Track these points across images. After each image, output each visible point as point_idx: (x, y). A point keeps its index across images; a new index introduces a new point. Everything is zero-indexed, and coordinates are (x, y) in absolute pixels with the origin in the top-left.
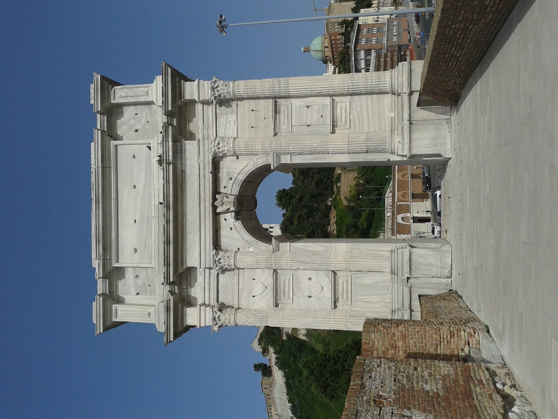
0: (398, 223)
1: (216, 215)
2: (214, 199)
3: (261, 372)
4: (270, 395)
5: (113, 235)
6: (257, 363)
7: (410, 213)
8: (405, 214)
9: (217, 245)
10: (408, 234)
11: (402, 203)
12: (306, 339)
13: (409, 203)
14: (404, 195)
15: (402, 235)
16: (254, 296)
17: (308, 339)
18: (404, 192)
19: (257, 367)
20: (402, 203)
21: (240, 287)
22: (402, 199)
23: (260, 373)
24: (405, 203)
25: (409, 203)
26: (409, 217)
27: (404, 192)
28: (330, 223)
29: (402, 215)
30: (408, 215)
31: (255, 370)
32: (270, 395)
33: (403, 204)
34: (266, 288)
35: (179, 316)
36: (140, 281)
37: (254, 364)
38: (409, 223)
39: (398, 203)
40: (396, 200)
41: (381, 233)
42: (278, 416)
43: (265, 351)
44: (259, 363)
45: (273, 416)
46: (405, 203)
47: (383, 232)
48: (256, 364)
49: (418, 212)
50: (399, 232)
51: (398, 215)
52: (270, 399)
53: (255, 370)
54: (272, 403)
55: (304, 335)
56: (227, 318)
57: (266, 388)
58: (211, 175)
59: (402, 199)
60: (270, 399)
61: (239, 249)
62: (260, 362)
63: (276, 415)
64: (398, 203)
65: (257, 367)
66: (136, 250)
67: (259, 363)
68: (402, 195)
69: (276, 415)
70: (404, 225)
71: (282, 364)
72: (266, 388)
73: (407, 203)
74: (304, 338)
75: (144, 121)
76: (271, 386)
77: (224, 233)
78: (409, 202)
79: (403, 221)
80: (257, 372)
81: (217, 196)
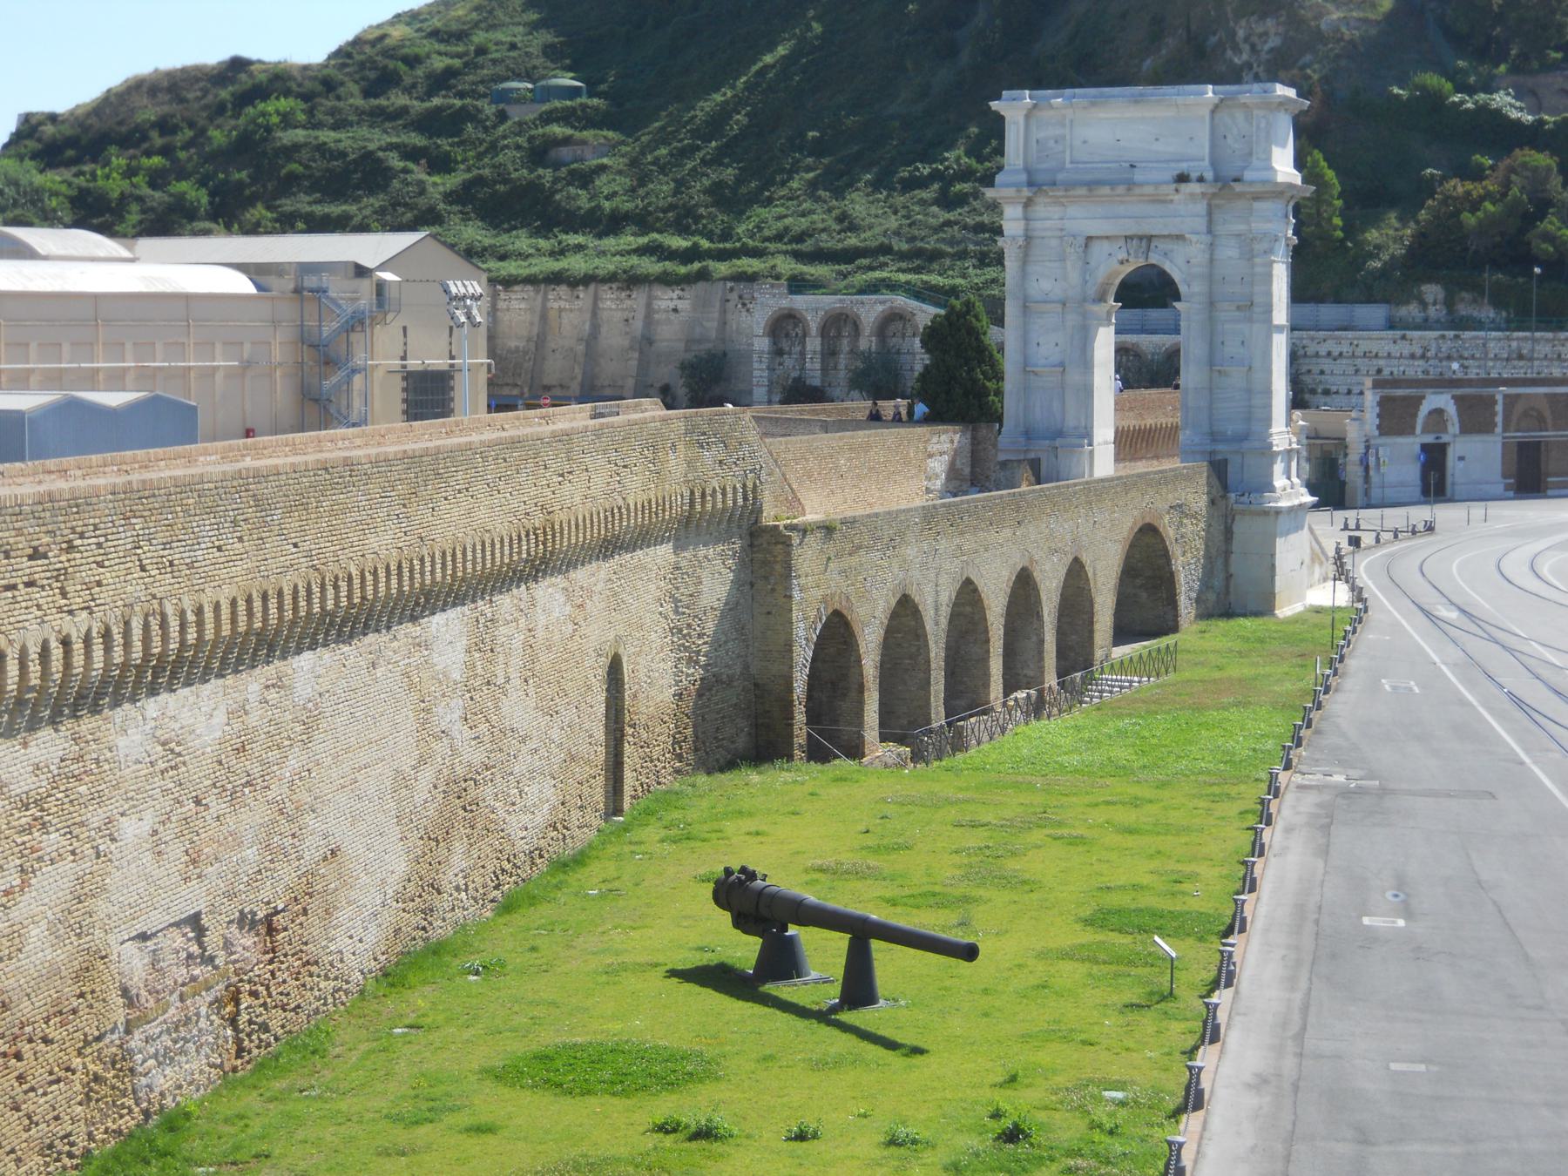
0: (1419, 400)
1: (1126, 237)
2: (1141, 238)
5: (1102, 115)
7: (1457, 431)
8: (1456, 420)
9: (1089, 239)
10: (1379, 427)
11: (1499, 408)
13: (1499, 429)
15: (1377, 410)
18: (1547, 414)
20: (1499, 408)
21: (1047, 264)
22: (1519, 408)
24: (1499, 419)
25: (1499, 429)
26: (1445, 430)
27: (1547, 414)
29: (1451, 409)
30: (1454, 427)
33: (1494, 414)
36: (1051, 143)
38: (1425, 431)
39: (1499, 398)
41: (1504, 314)
46: (1499, 419)
47: (1508, 321)
49: (1461, 458)
50: (1384, 403)
51: (1453, 397)
58: (1166, 233)
59: (1519, 408)
64: (1499, 398)
66: (1085, 142)
68: (1532, 409)
70: (1415, 415)
73: (1500, 425)
75: (1236, 146)
78: (1505, 430)
79: (1430, 413)
81: (1144, 241)
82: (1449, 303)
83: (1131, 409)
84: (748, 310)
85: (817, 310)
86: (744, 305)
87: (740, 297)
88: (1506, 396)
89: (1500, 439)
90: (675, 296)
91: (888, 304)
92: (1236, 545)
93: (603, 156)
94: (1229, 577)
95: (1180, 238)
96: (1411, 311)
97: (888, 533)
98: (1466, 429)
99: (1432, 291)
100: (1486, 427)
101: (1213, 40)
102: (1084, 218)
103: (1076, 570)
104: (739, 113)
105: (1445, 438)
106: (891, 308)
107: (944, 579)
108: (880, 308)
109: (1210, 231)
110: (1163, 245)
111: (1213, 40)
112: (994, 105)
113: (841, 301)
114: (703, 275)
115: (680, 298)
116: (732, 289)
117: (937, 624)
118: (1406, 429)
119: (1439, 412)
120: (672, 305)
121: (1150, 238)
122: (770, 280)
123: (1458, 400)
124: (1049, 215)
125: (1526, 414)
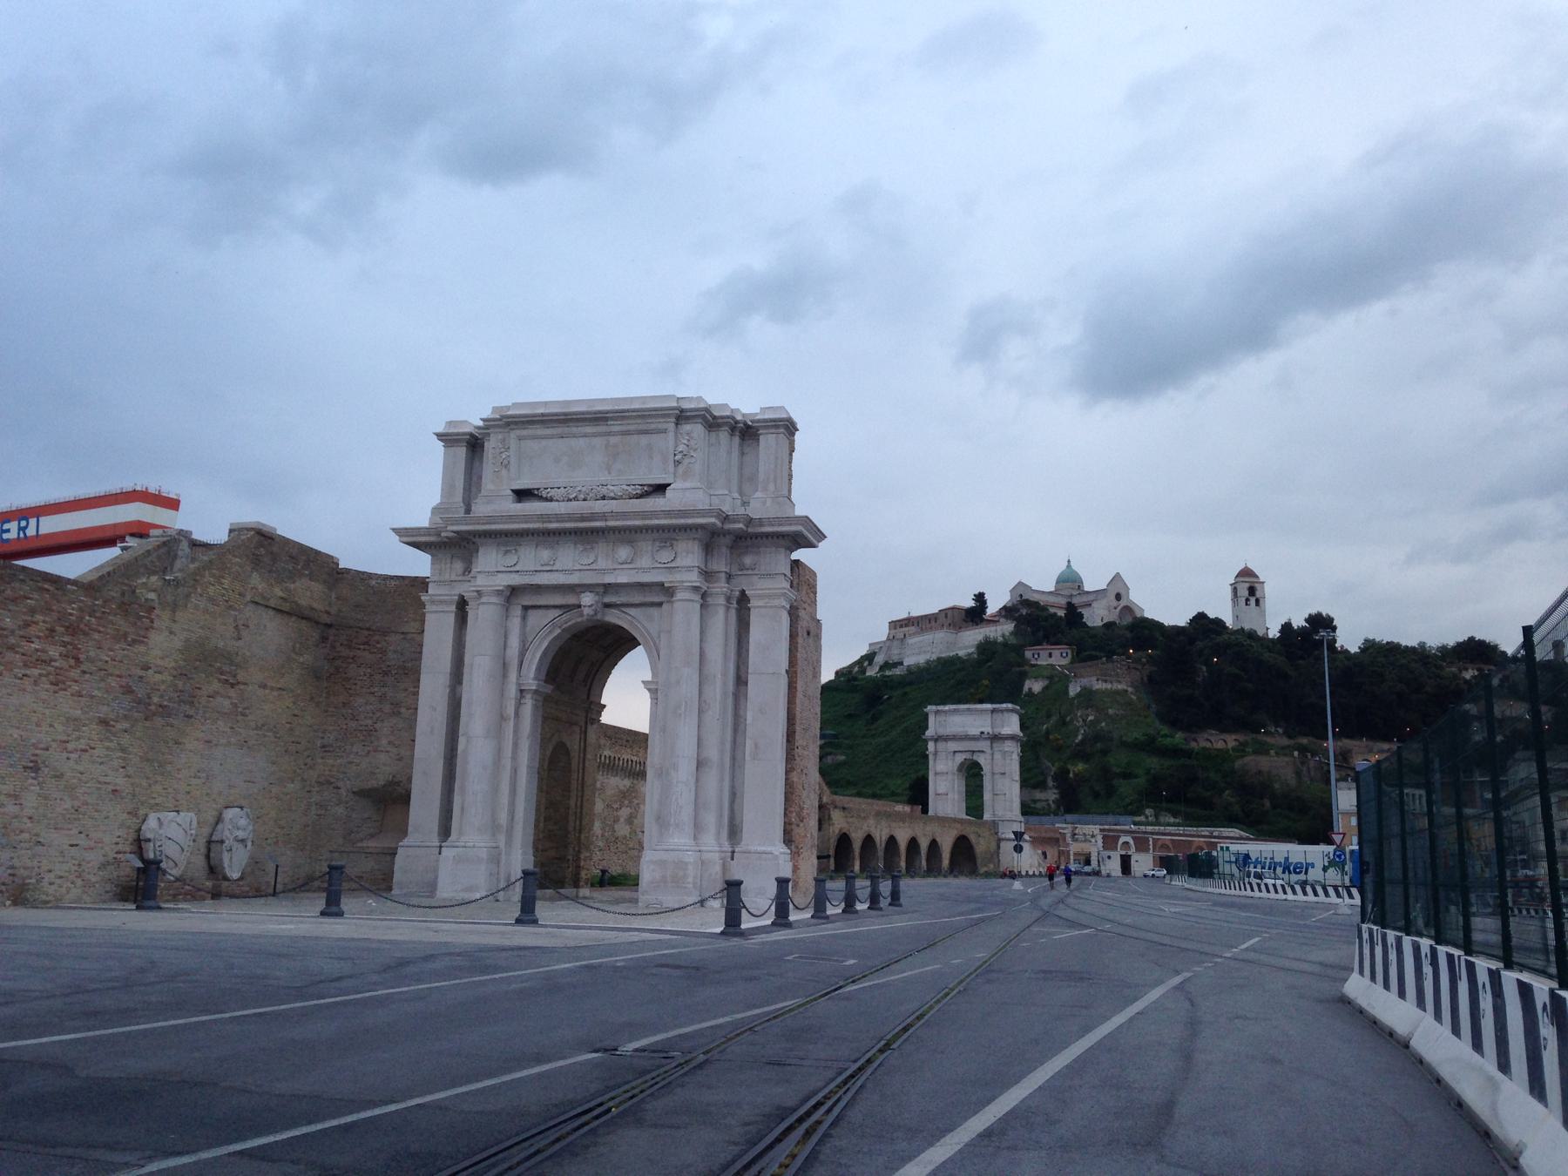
4: (936, 622)
9: (955, 752)
11: (1151, 843)
14: (1164, 847)
18: (1171, 846)
19: (980, 598)
20: (1151, 843)
24: (1151, 847)
27: (1171, 846)
28: (1224, 734)
29: (1132, 842)
31: (975, 595)
32: (936, 622)
33: (1149, 845)
35: (931, 740)
39: (1151, 839)
40: (1154, 837)
43: (1007, 612)
45: (902, 630)
46: (1151, 847)
50: (1104, 838)
52: (930, 622)
53: (975, 595)
54: (924, 627)
55: (1030, 689)
56: (931, 757)
57: (946, 617)
59: (1160, 843)
60: (930, 622)
63: (905, 635)
65: (980, 598)
69: (905, 635)
71: (986, 648)
72: (946, 617)
74: (1026, 688)
76: (950, 625)
77: (960, 754)
79: (1124, 843)
82: (1156, 816)
88: (1153, 839)
89: (1152, 855)
92: (1001, 851)
94: (999, 861)
95: (983, 751)
96: (1142, 818)
97: (862, 815)
98: (1138, 850)
99: (1148, 812)
100: (1147, 850)
101: (1068, 718)
102: (952, 746)
103: (934, 845)
105: (1129, 854)
107: (884, 833)
109: (992, 748)
110: (979, 754)
111: (1068, 718)
112: (925, 710)
117: (881, 845)
118: (1115, 849)
119: (1127, 843)
121: (974, 752)
123: (1132, 838)
124: (941, 745)
125: (1162, 846)
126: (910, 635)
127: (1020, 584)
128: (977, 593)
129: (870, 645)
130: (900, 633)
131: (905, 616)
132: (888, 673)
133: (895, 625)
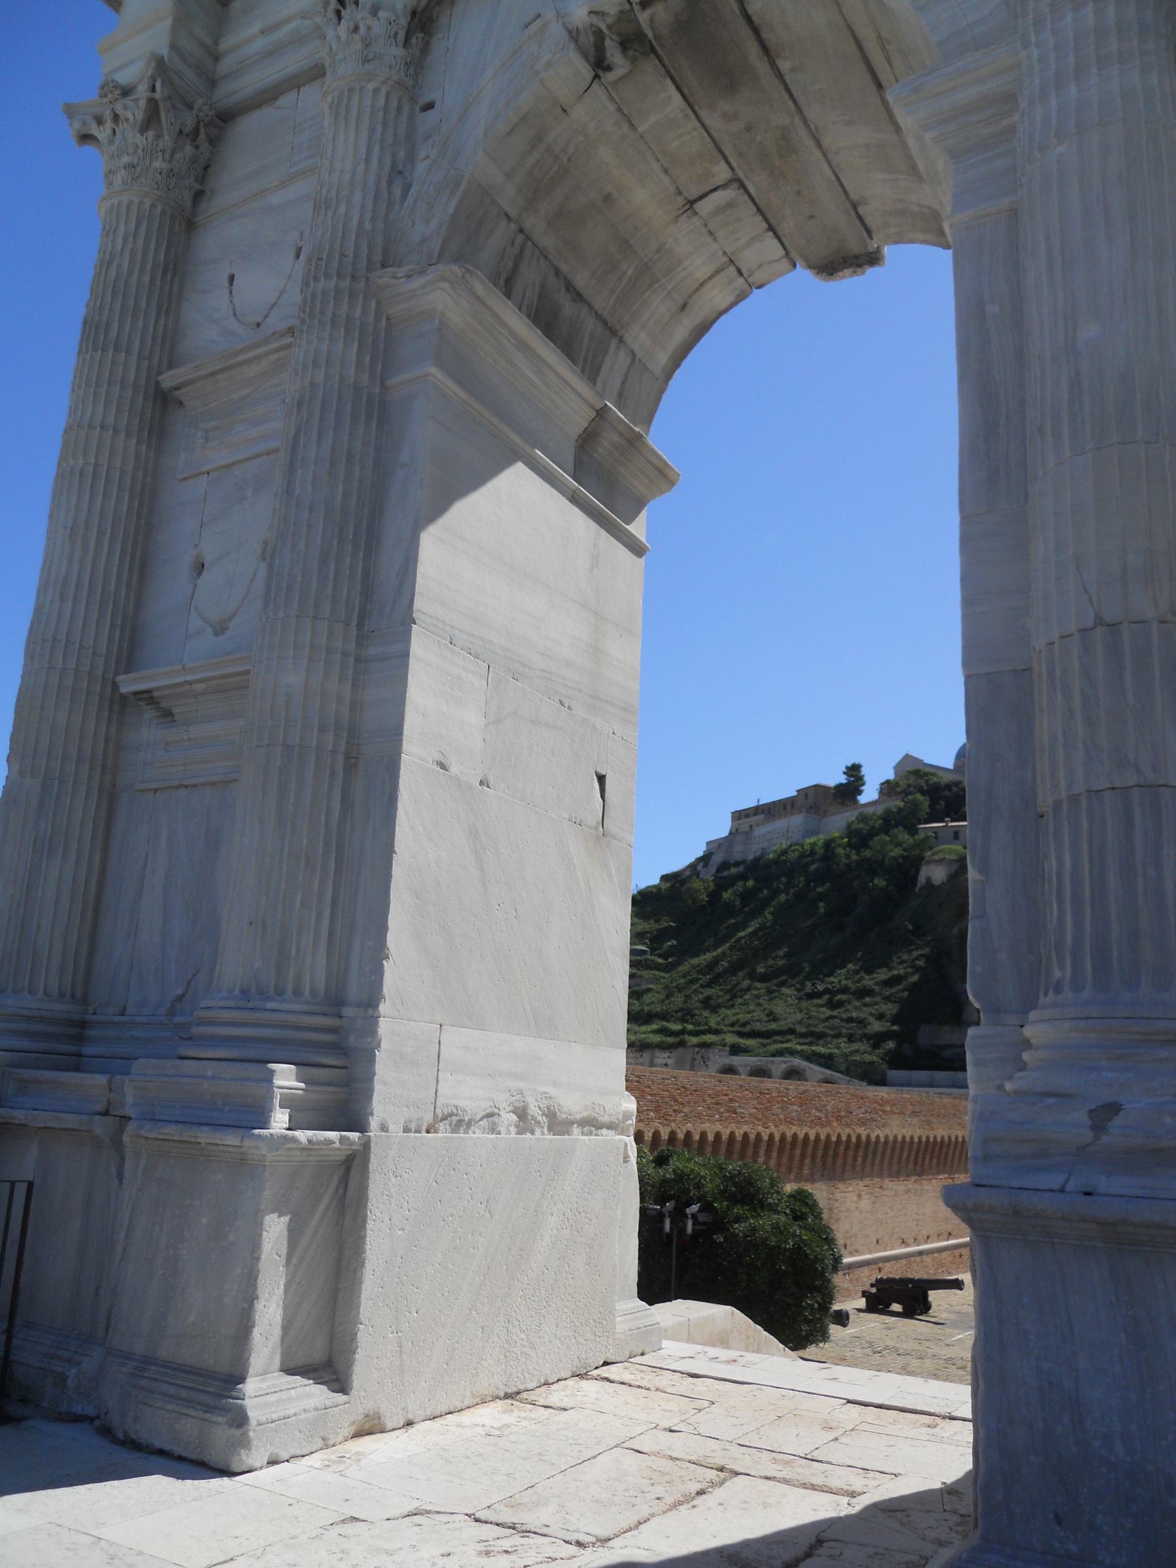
3: (844, 781)
6: (864, 771)
12: (919, 885)
16: (232, 278)
17: (920, 889)
19: (854, 771)
23: (843, 779)
31: (847, 768)
34: (258, 325)
37: (861, 763)
42: (748, 829)
44: (863, 776)
45: (748, 820)
48: (862, 769)
53: (847, 768)
55: (929, 879)
61: (430, 106)
62: (866, 779)
63: (751, 826)
65: (854, 771)
67: (863, 776)
69: (751, 826)
74: (922, 879)
76: (811, 808)
80: (844, 773)
83: (914, 1114)
84: (706, 1066)
85: (746, 1066)
86: (704, 1062)
87: (703, 1057)
90: (666, 1056)
91: (789, 1064)
93: (651, 984)
104: (723, 961)
106: (791, 1066)
108: (784, 1066)
113: (760, 1061)
114: (682, 1044)
115: (669, 1057)
116: (698, 1052)
120: (664, 1061)
122: (720, 1047)
126: (758, 825)
127: (907, 757)
128: (849, 765)
129: (708, 843)
130: (744, 825)
131: (753, 804)
132: (726, 873)
133: (738, 816)
